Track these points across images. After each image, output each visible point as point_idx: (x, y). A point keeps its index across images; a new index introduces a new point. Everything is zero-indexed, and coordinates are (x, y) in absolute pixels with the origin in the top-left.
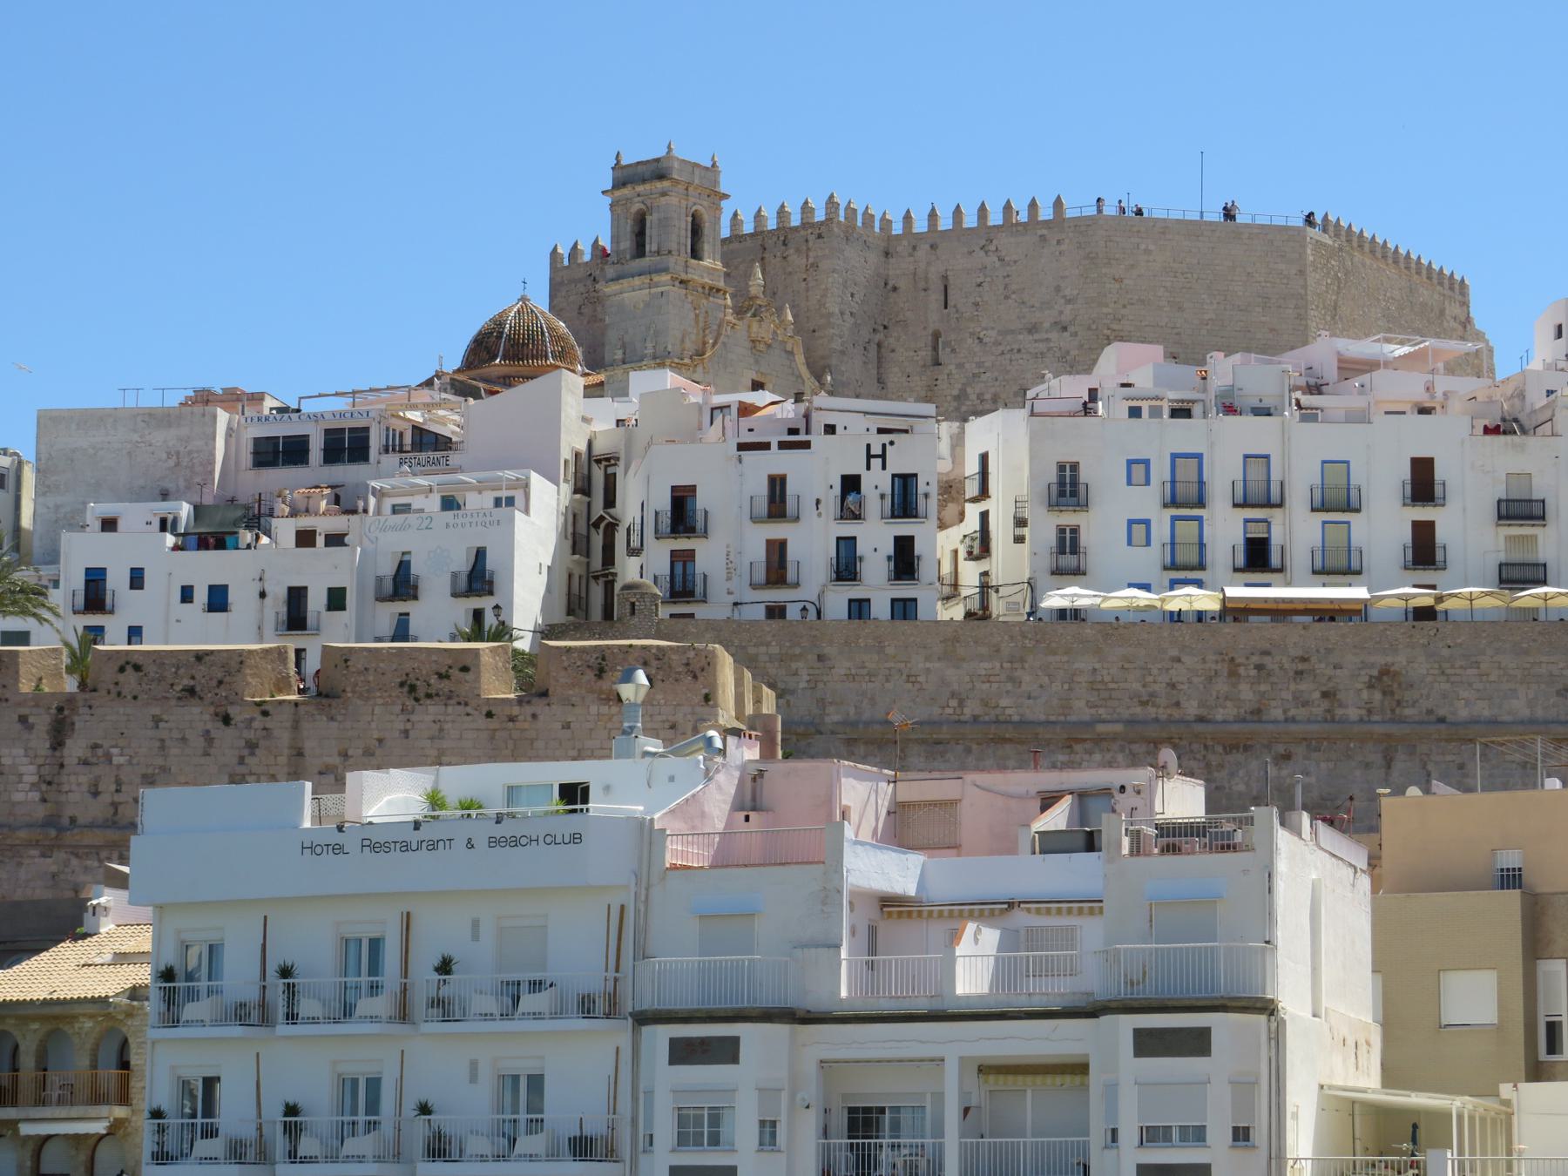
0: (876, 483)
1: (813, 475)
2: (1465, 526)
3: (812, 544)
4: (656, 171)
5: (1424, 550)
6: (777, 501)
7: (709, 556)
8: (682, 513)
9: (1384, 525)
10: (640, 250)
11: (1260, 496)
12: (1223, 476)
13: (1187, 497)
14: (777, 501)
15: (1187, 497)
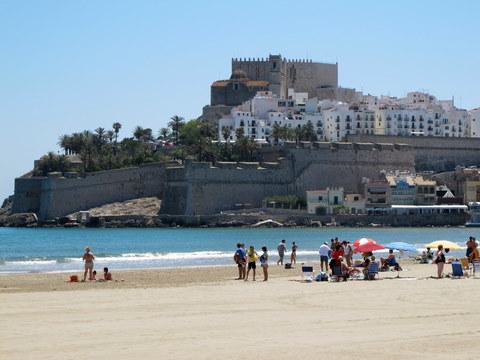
0: (369, 117)
1: (362, 115)
2: (426, 125)
3: (362, 123)
4: (278, 57)
5: (421, 127)
6: (359, 118)
7: (351, 124)
8: (348, 119)
9: (417, 124)
10: (275, 66)
11: (407, 120)
12: (403, 117)
13: (400, 119)
14: (359, 118)
15: (400, 119)
